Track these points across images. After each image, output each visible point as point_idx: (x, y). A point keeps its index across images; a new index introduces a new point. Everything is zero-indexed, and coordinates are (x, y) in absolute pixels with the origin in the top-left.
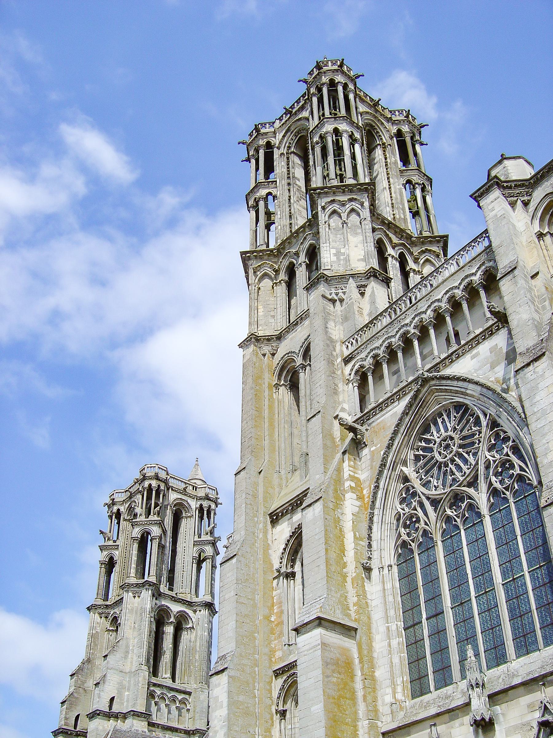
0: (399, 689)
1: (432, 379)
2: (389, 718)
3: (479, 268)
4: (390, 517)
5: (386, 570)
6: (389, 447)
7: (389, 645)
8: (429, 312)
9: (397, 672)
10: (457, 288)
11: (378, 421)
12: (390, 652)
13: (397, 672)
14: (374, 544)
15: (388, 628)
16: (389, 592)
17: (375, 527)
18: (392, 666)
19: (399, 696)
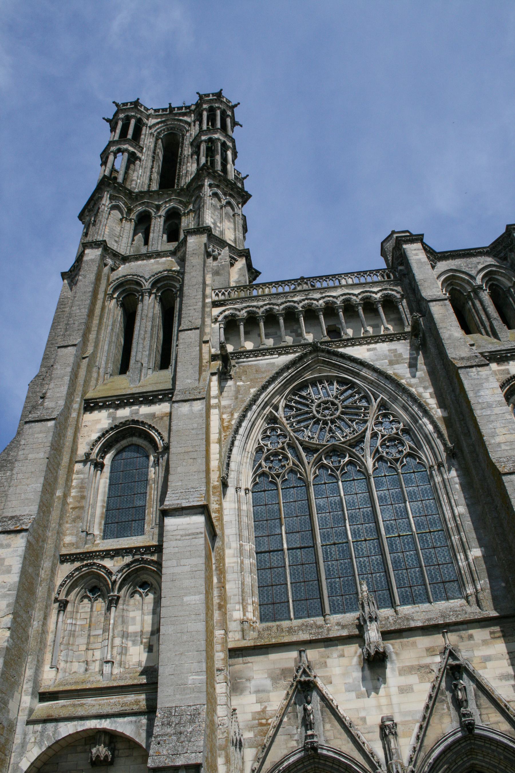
0: (250, 608)
1: (323, 351)
2: (238, 636)
3: (381, 291)
4: (251, 446)
5: (243, 493)
6: (264, 388)
7: (242, 562)
8: (321, 302)
9: (248, 590)
10: (356, 295)
11: (250, 363)
12: (242, 570)
13: (248, 590)
14: (233, 466)
15: (241, 546)
16: (244, 513)
17: (235, 450)
18: (243, 584)
19: (250, 615)
